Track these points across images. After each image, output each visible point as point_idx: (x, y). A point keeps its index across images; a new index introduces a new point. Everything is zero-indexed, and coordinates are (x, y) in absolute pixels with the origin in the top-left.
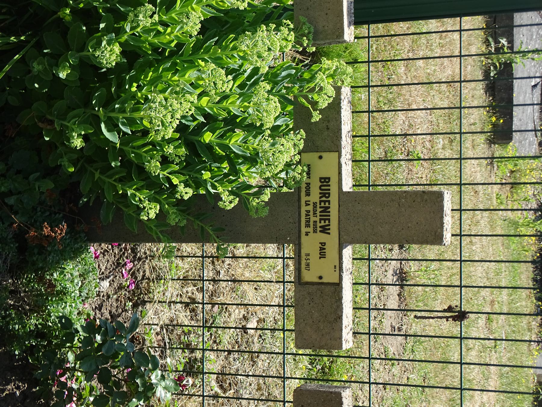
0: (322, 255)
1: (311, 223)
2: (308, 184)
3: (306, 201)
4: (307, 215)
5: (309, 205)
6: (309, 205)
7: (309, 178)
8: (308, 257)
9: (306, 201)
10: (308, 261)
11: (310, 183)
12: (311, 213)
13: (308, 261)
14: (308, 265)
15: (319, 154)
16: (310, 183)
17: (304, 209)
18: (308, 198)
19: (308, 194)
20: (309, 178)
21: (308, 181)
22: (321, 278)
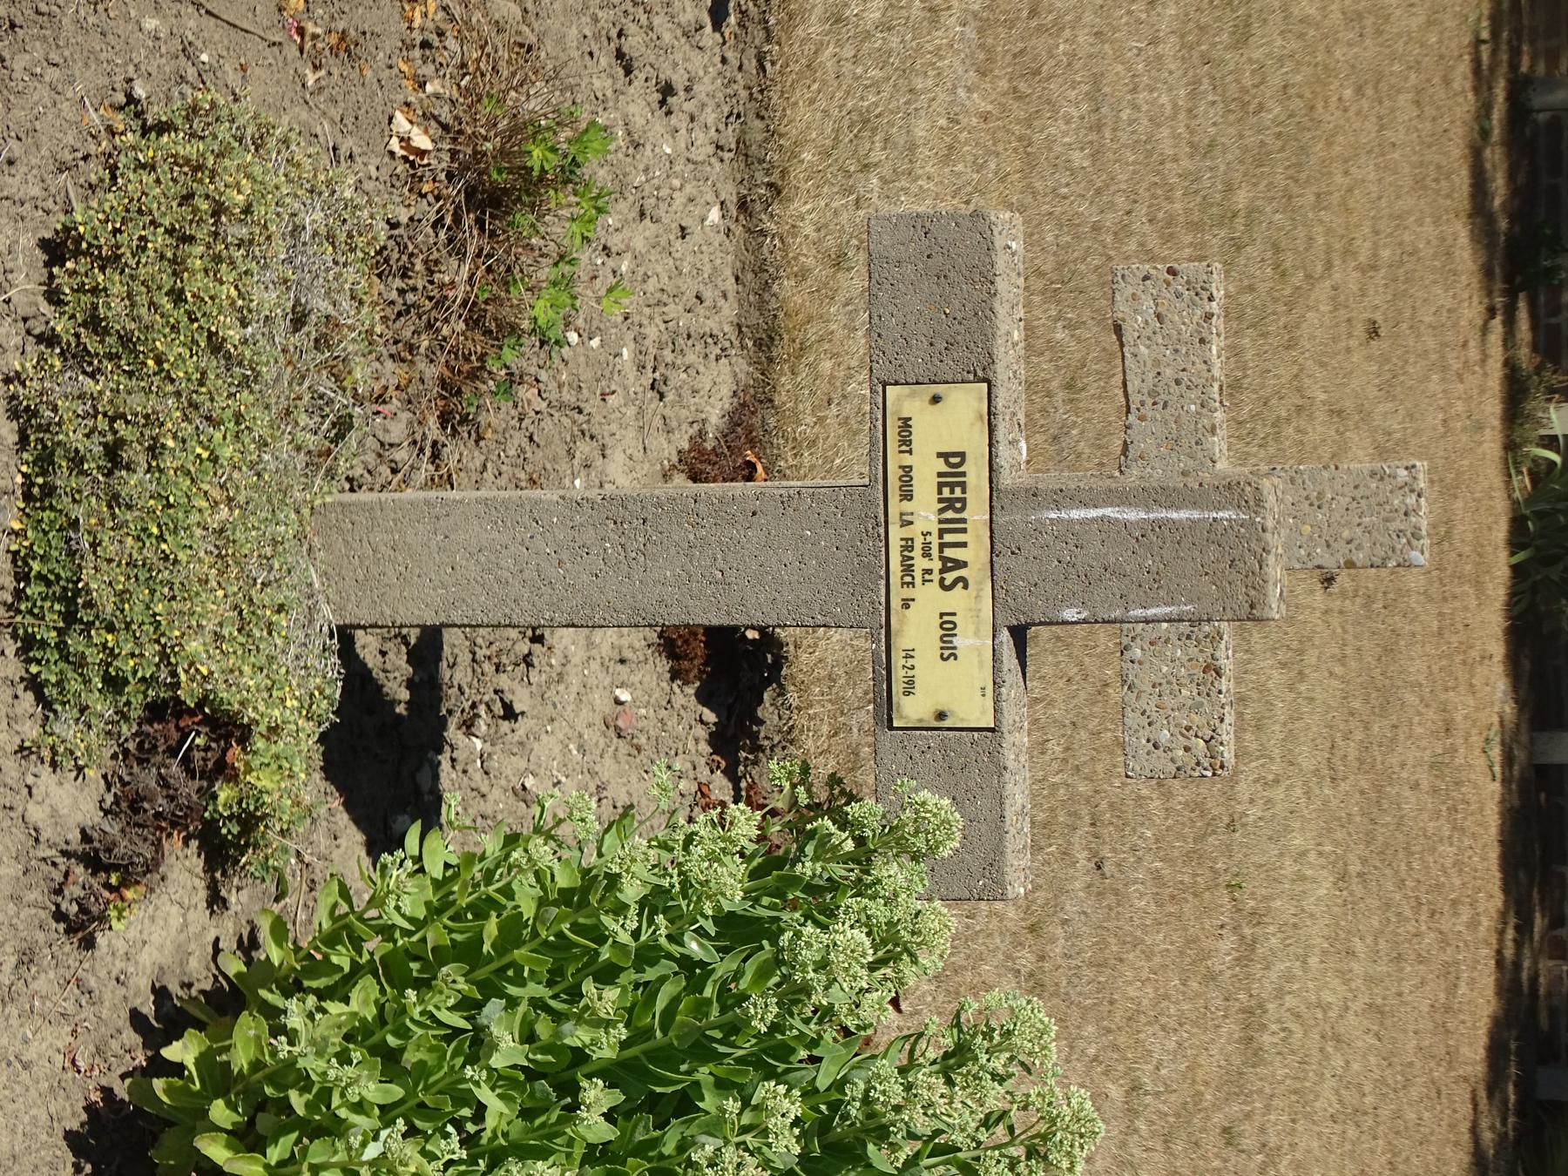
0: (948, 652)
1: (918, 574)
2: (907, 470)
7: (910, 452)
8: (910, 662)
10: (910, 673)
12: (918, 545)
13: (910, 673)
14: (910, 682)
15: (939, 389)
17: (896, 534)
18: (907, 506)
19: (907, 496)
20: (910, 452)
21: (907, 460)
22: (941, 716)
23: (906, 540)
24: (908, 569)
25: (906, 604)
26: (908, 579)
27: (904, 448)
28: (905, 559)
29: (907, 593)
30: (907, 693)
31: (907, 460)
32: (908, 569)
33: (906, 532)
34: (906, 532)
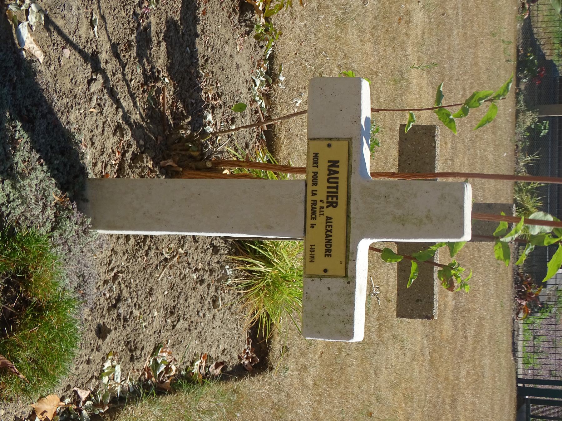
1: (318, 213)
2: (316, 173)
3: (312, 191)
4: (313, 204)
5: (316, 194)
6: (316, 194)
7: (317, 167)
9: (312, 191)
10: (313, 253)
11: (317, 173)
13: (313, 253)
15: (329, 142)
16: (317, 173)
17: (310, 198)
18: (314, 188)
19: (315, 183)
20: (317, 167)
21: (315, 169)
23: (314, 201)
24: (314, 213)
25: (312, 226)
26: (314, 216)
27: (315, 165)
28: (313, 208)
29: (313, 222)
30: (311, 262)
31: (315, 169)
32: (314, 213)
33: (314, 198)
34: (314, 198)
